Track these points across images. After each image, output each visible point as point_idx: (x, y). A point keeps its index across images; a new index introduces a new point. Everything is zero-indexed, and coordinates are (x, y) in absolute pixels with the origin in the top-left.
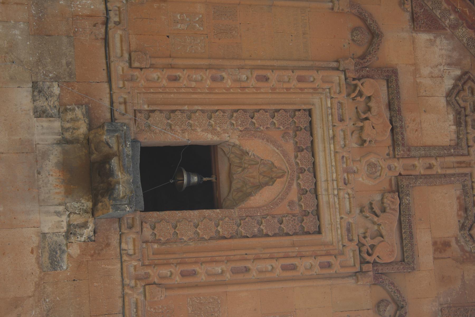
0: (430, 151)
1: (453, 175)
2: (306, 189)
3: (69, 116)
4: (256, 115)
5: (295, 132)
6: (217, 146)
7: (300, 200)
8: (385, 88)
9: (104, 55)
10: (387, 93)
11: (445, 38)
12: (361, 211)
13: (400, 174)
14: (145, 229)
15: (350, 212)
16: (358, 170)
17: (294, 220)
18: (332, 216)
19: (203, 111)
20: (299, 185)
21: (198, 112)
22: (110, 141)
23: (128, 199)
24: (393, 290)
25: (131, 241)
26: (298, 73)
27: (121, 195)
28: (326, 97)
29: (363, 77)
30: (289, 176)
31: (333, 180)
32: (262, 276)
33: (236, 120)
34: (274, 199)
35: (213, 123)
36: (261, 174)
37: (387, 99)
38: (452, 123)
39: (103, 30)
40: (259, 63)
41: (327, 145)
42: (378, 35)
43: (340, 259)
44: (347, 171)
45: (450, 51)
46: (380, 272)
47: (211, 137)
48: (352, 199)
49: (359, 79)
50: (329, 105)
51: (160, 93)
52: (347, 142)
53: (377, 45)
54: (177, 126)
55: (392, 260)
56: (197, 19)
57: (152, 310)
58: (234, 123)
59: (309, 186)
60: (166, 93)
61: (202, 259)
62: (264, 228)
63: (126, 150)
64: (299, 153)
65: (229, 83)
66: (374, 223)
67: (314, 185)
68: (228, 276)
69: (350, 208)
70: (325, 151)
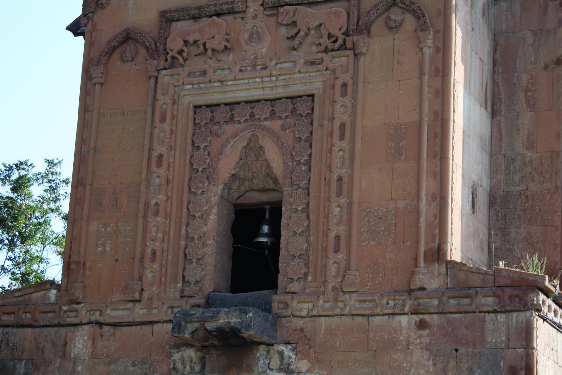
3: (179, 366)
4: (195, 166)
6: (235, 205)
8: (179, 23)
9: (128, 328)
10: (184, 22)
12: (295, 49)
13: (262, 5)
15: (294, 62)
16: (254, 54)
17: (298, 124)
18: (297, 82)
19: (187, 225)
20: (266, 119)
22: (190, 330)
24: (375, 11)
26: (157, 123)
27: (239, 320)
28: (183, 89)
29: (165, 50)
30: (257, 130)
31: (263, 82)
32: (347, 162)
33: (198, 189)
35: (199, 213)
36: (258, 159)
37: (189, 21)
39: (107, 328)
40: (145, 164)
41: (228, 89)
42: (128, 33)
43: (339, 74)
44: (254, 66)
48: (281, 61)
50: (190, 86)
51: (166, 271)
52: (226, 66)
54: (199, 253)
55: (344, 13)
56: (103, 229)
57: (369, 284)
58: (200, 191)
59: (267, 109)
60: (167, 264)
62: (303, 159)
63: (198, 315)
64: (235, 119)
65: (161, 197)
66: (307, 35)
68: (343, 200)
69: (291, 62)
70: (234, 91)
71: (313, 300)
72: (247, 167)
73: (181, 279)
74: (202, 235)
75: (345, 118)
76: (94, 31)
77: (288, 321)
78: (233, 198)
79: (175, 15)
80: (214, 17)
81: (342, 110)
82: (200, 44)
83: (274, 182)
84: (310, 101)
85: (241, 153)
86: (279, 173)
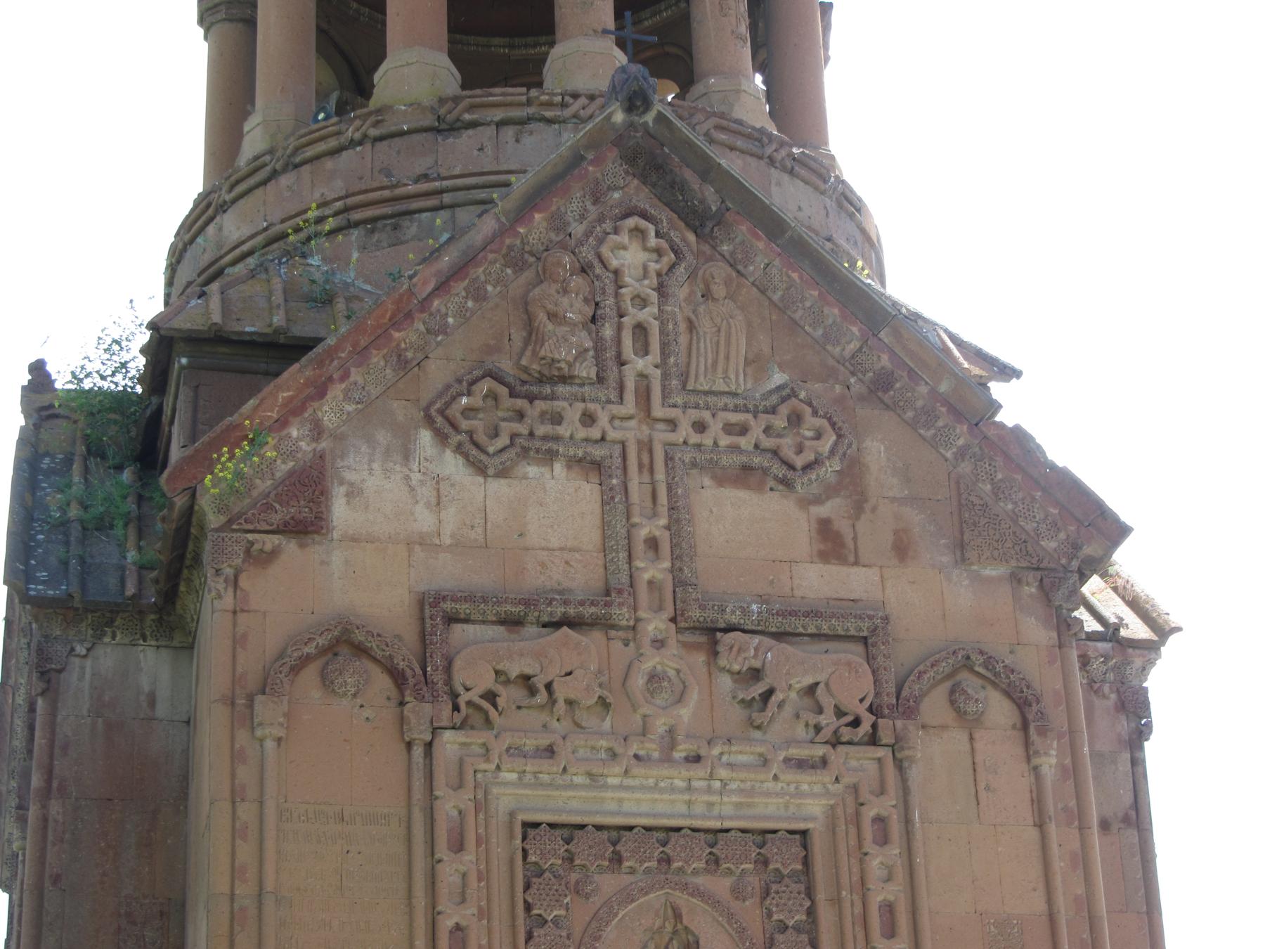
0: (616, 540)
1: (670, 488)
7: (730, 872)
8: (470, 629)
11: (342, 458)
13: (673, 620)
20: (695, 872)
26: (442, 851)
29: (449, 681)
30: (678, 893)
31: (689, 789)
37: (495, 627)
38: (545, 470)
43: (865, 795)
45: (374, 449)
46: (894, 701)
49: (454, 696)
50: (514, 776)
53: (370, 638)
67: (697, 834)
75: (894, 892)
76: (243, 611)
79: (463, 608)
80: (565, 628)
82: (540, 683)
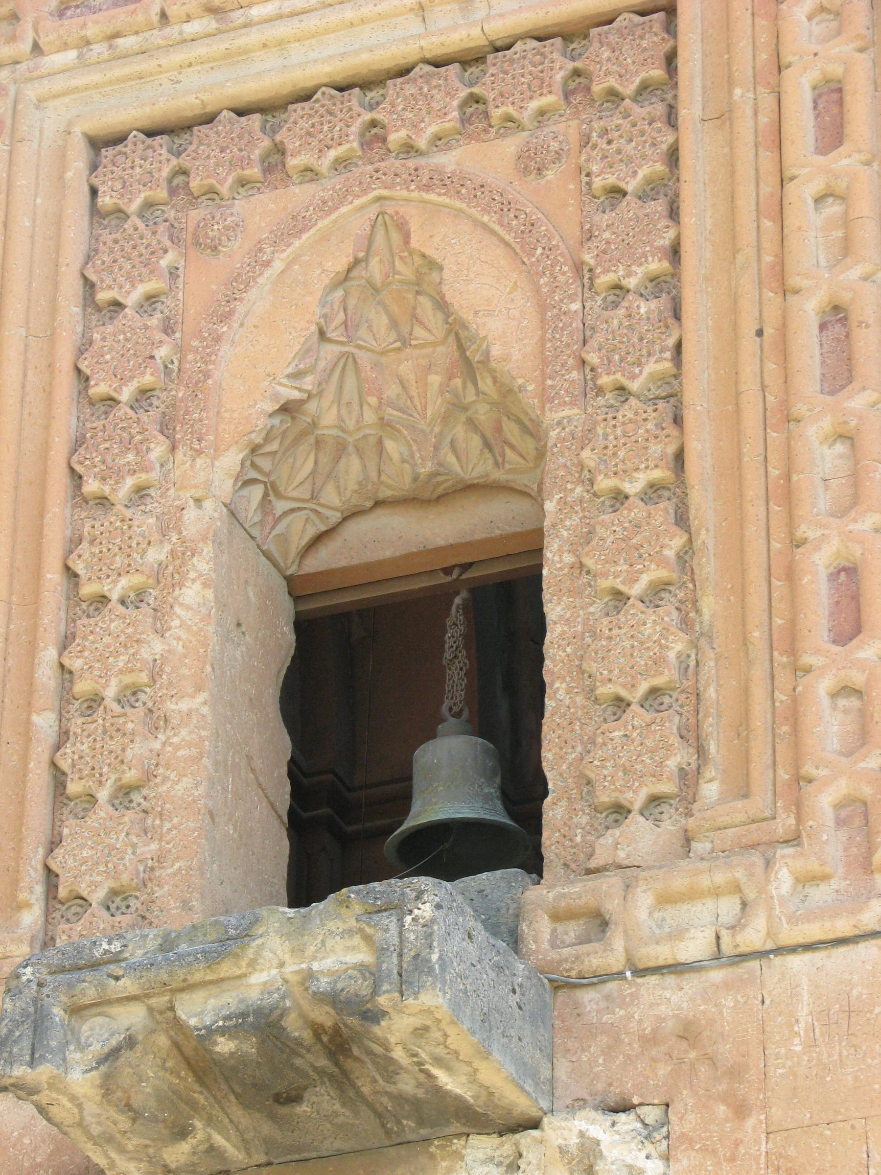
2: (464, 104)
5: (194, 199)
14: (622, 854)
21: (66, 662)
22: (97, 1048)
23: (376, 917)
25: (674, 915)
27: (364, 956)
30: (400, 193)
33: (119, 475)
34: (507, 244)
35: (124, 582)
36: (405, 342)
47: (197, 586)
50: (71, 55)
54: (129, 753)
58: (130, 482)
61: (776, 545)
70: (281, 44)
71: (740, 874)
72: (351, 383)
73: (39, 889)
74: (144, 678)
77: (608, 997)
78: (283, 539)
81: (817, 30)
83: (487, 444)
84: (657, 27)
85: (323, 303)
86: (516, 356)
